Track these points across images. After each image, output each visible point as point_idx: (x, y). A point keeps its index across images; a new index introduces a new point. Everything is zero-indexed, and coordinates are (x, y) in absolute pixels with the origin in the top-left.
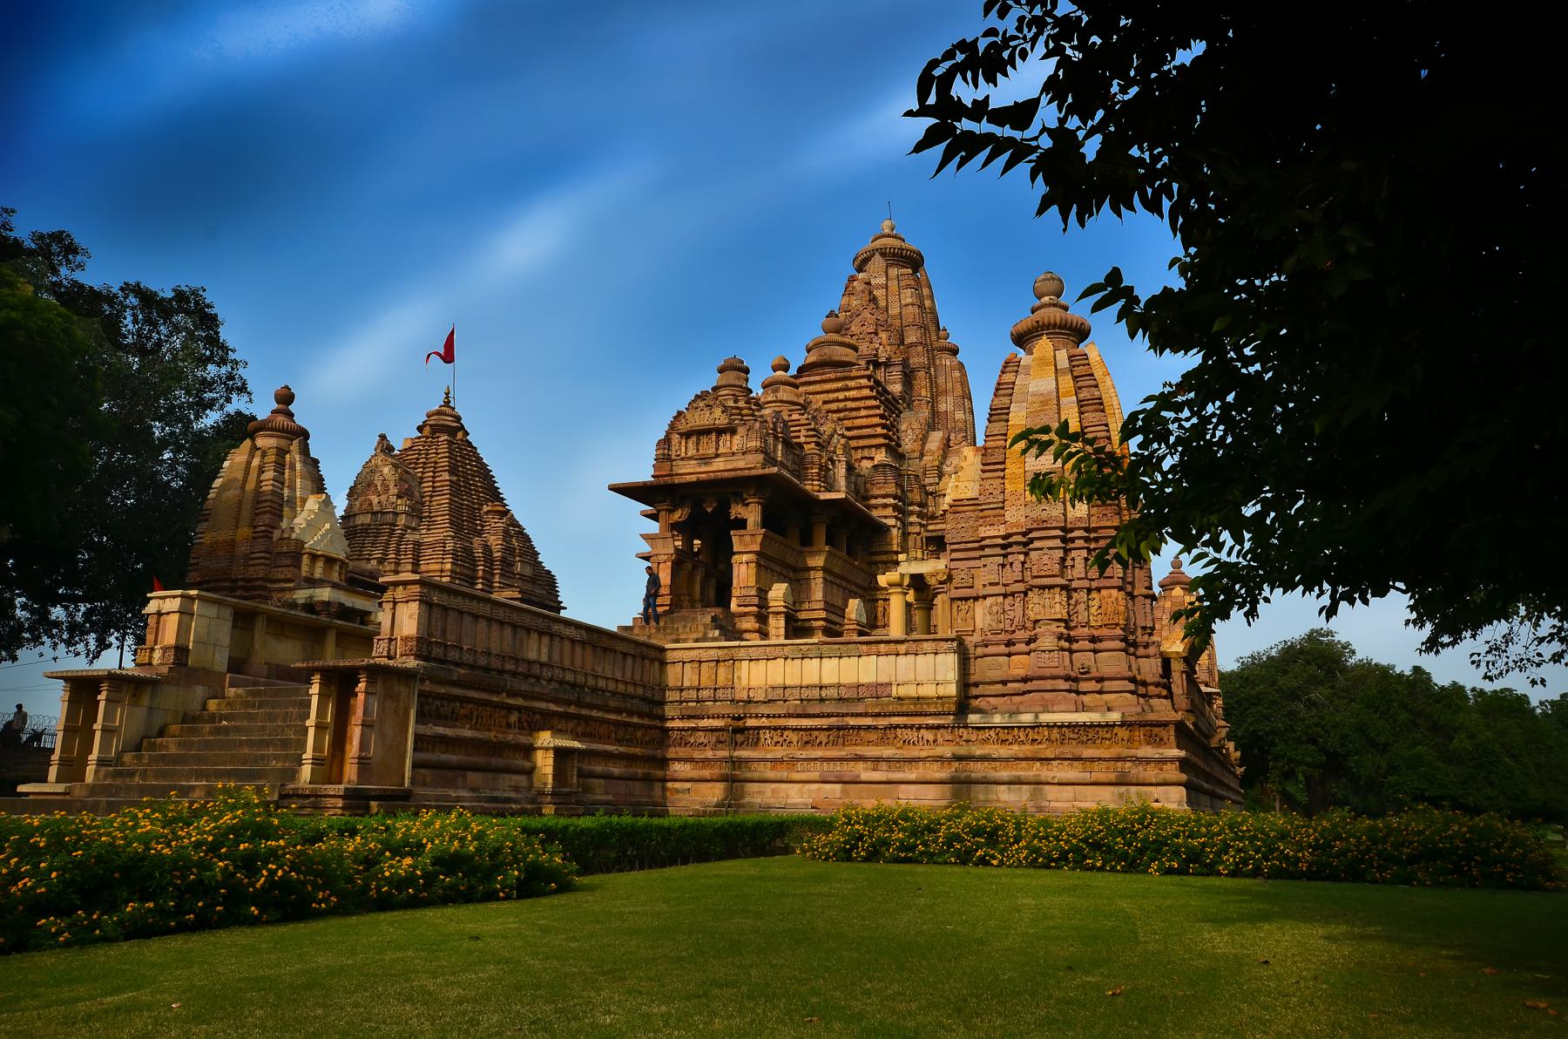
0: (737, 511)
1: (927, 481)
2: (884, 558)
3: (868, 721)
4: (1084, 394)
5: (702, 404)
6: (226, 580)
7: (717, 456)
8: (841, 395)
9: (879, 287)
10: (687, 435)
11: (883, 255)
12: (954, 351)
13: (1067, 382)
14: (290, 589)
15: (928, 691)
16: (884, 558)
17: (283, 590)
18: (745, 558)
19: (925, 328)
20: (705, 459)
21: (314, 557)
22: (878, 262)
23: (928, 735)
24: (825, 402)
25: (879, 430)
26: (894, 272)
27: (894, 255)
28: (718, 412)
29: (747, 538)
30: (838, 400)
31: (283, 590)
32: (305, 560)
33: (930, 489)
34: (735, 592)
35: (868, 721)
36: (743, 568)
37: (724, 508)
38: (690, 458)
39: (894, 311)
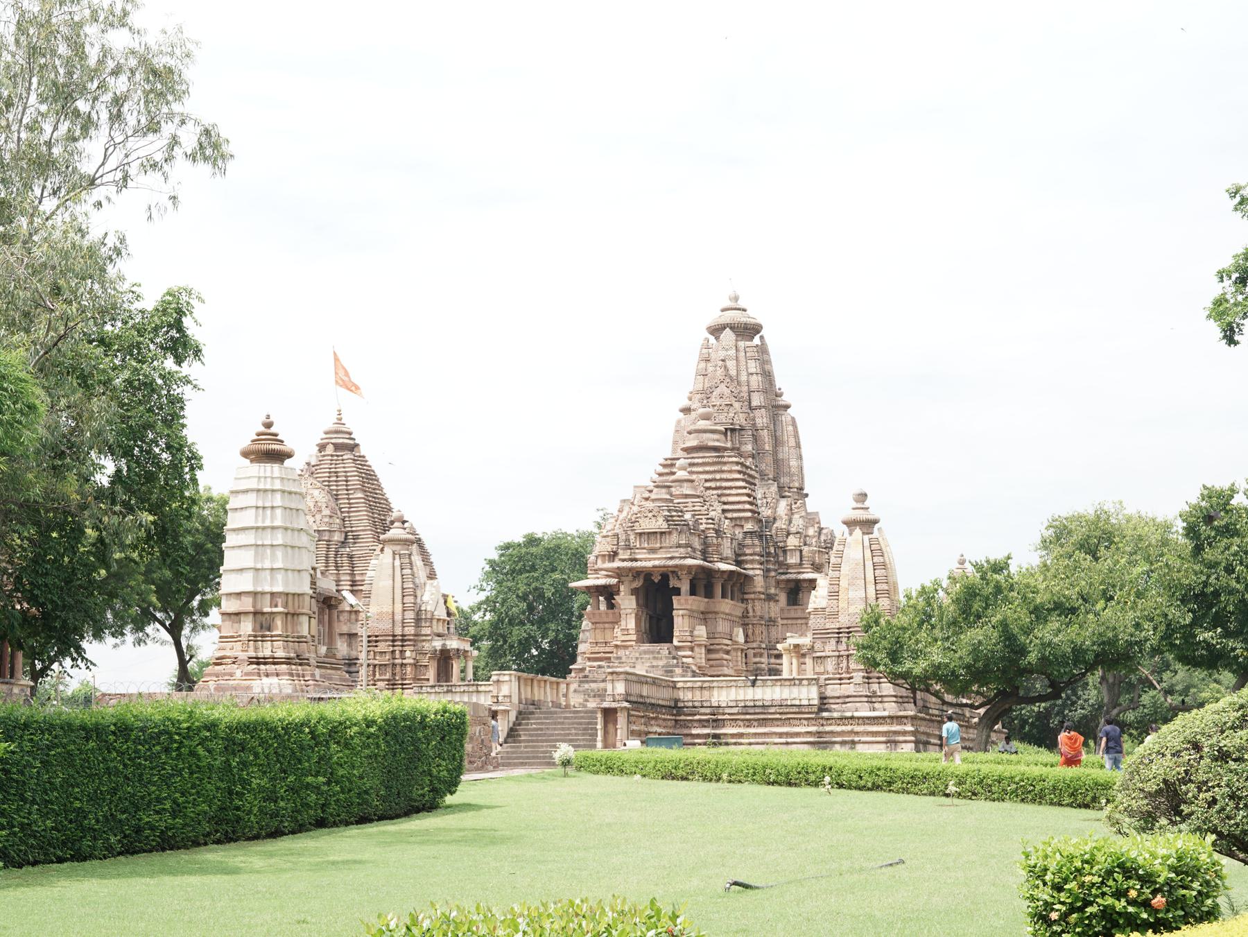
0: (673, 583)
2: (752, 596)
3: (778, 716)
4: (876, 559)
5: (650, 515)
8: (718, 476)
9: (730, 358)
13: (868, 554)
15: (805, 702)
16: (752, 596)
18: (681, 612)
19: (765, 391)
22: (728, 335)
23: (805, 722)
24: (706, 481)
25: (748, 506)
26: (742, 344)
28: (661, 520)
30: (715, 480)
32: (435, 622)
35: (778, 716)
39: (744, 378)
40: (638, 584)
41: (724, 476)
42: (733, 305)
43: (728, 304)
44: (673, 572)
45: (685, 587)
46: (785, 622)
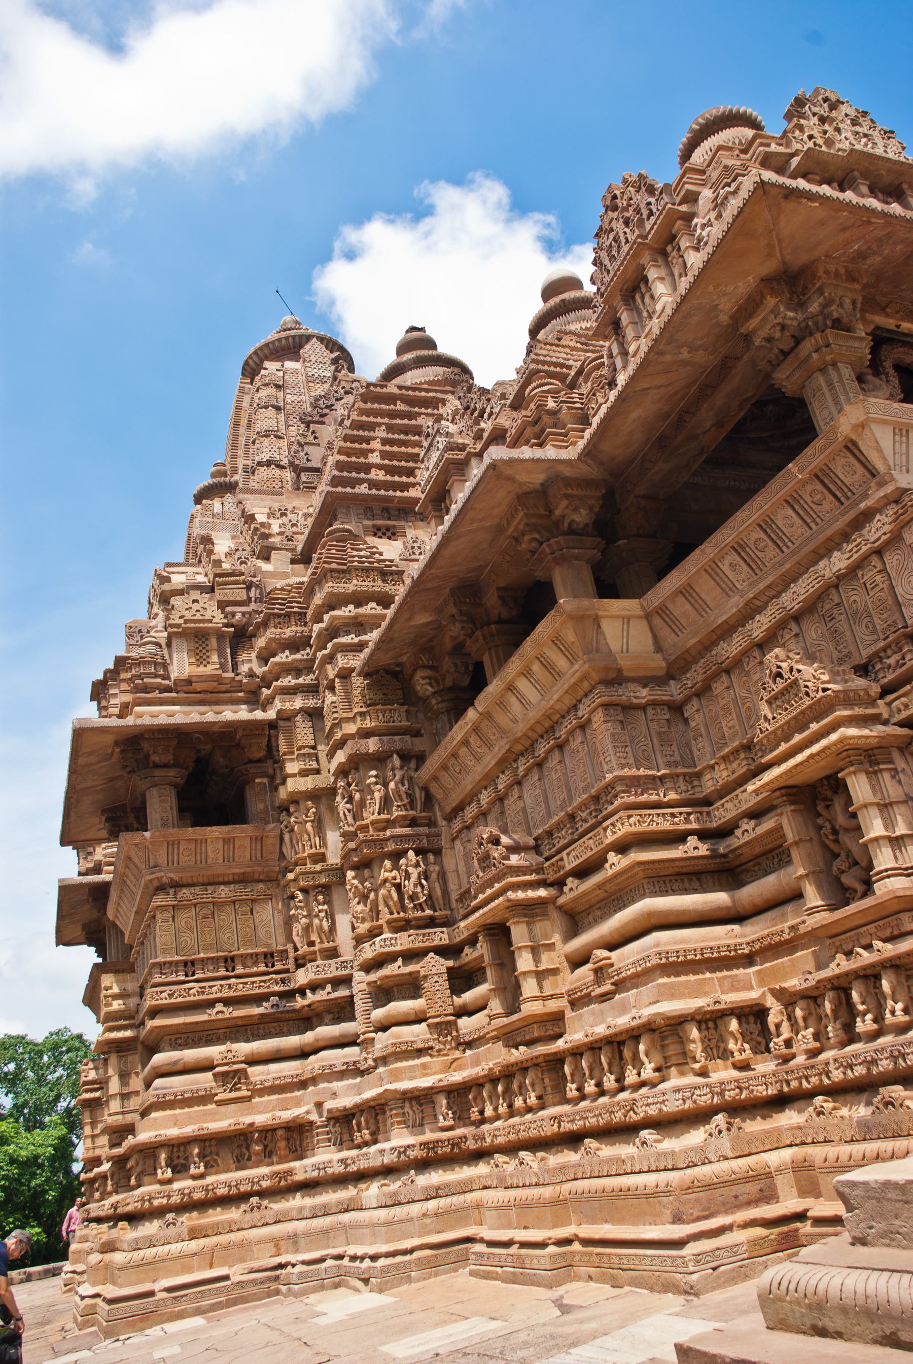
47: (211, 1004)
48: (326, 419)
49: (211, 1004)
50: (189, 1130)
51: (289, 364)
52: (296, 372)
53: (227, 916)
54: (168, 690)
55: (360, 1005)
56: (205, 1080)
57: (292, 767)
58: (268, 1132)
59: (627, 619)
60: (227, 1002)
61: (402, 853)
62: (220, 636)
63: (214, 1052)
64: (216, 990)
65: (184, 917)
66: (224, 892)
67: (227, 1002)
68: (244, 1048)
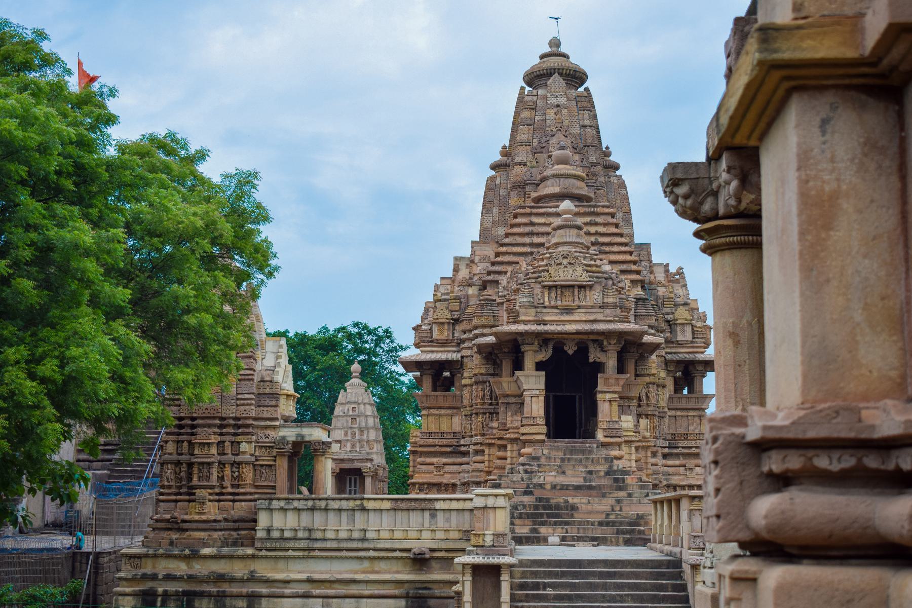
0: (594, 355)
1: (666, 310)
5: (565, 262)
6: (214, 418)
7: (579, 307)
10: (550, 288)
11: (561, 74)
12: (616, 167)
14: (274, 427)
17: (267, 427)
18: (608, 396)
20: (568, 310)
21: (288, 396)
27: (568, 75)
28: (580, 270)
29: (612, 381)
31: (267, 427)
32: (282, 400)
33: (669, 317)
34: (600, 425)
36: (607, 404)
37: (583, 350)
38: (553, 307)
40: (544, 355)
41: (601, 229)
42: (554, 49)
43: (548, 49)
44: (594, 341)
45: (611, 363)
46: (673, 413)
47: (435, 446)
48: (544, 150)
49: (435, 446)
50: (425, 481)
51: (541, 92)
52: (545, 97)
53: (444, 419)
54: (431, 341)
55: (471, 455)
56: (431, 468)
57: (466, 374)
58: (447, 485)
59: (510, 382)
60: (440, 446)
61: (485, 413)
62: (449, 323)
63: (434, 460)
64: (438, 442)
65: (430, 418)
66: (443, 412)
67: (440, 446)
68: (444, 460)
